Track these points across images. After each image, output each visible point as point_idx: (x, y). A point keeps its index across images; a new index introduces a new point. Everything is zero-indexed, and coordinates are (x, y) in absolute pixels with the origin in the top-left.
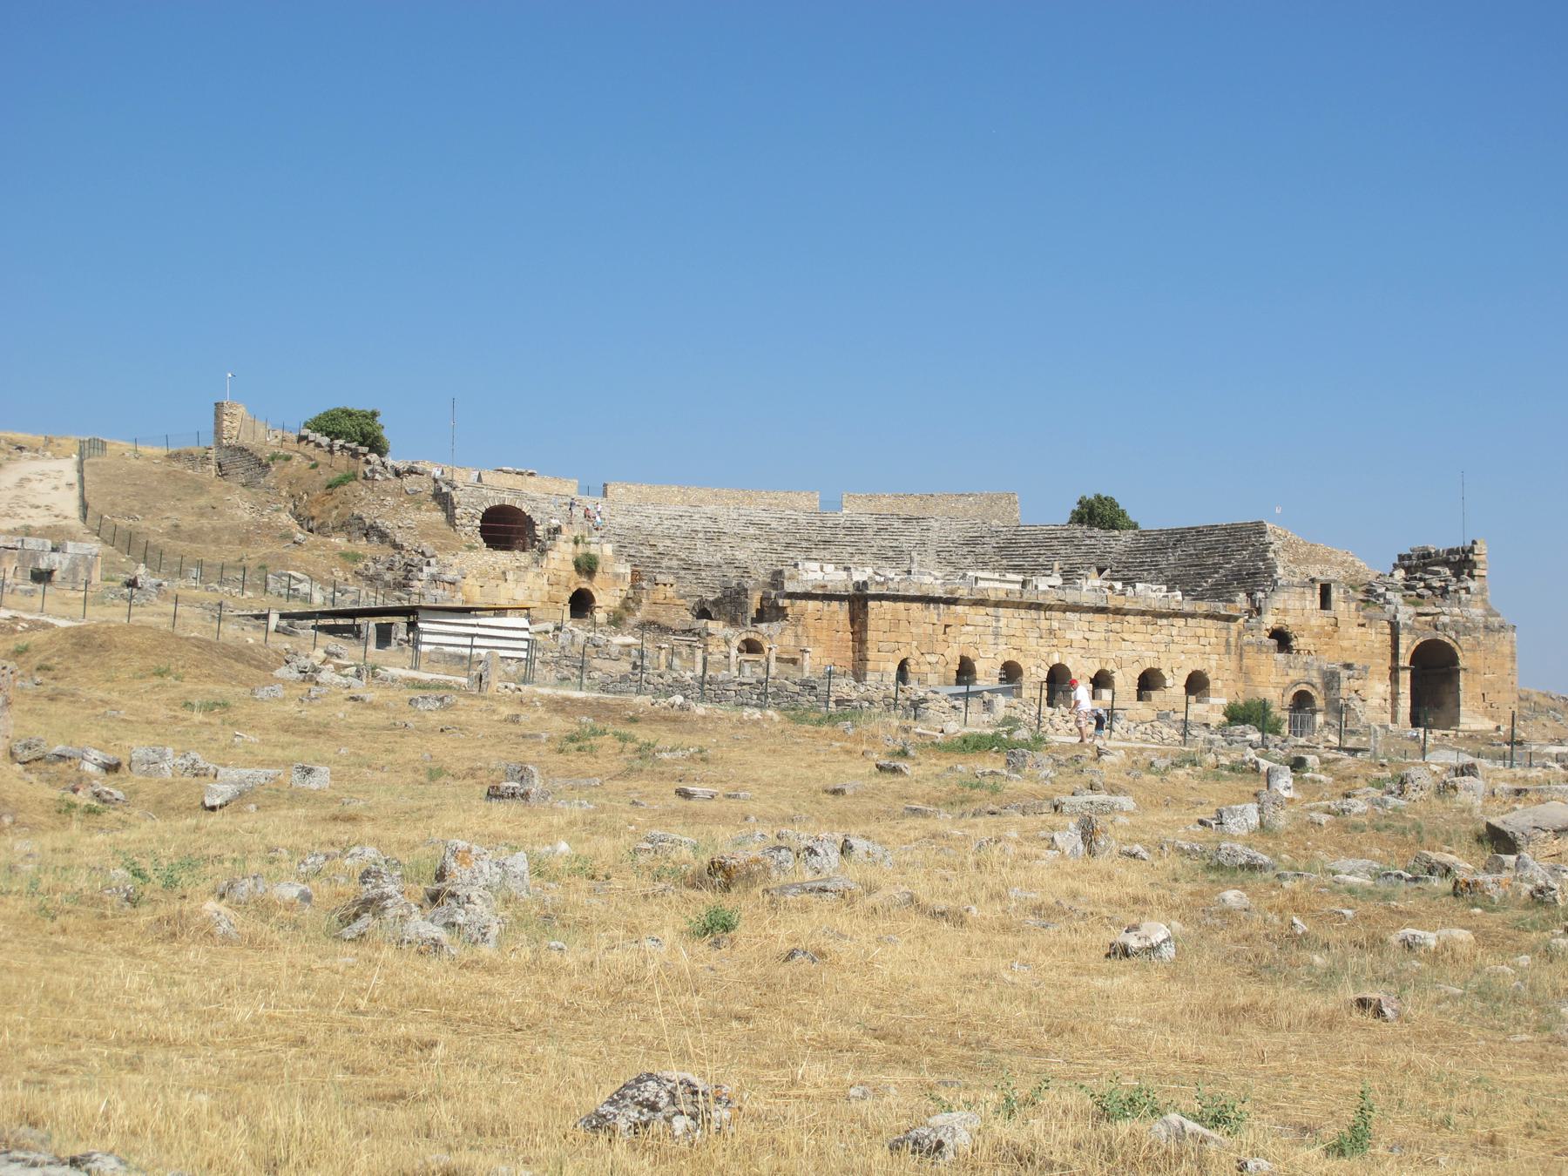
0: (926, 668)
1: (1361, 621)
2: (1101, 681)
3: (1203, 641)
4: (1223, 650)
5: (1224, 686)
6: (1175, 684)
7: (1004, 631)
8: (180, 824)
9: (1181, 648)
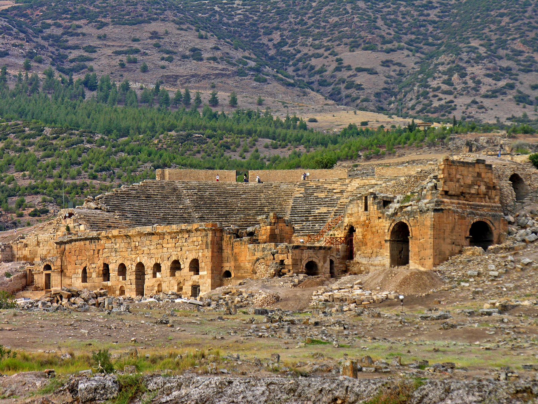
0: (92, 270)
1: (380, 215)
2: (157, 267)
3: (196, 244)
4: (204, 247)
5: (206, 265)
6: (185, 265)
7: (118, 250)
8: (40, 351)
9: (187, 248)
